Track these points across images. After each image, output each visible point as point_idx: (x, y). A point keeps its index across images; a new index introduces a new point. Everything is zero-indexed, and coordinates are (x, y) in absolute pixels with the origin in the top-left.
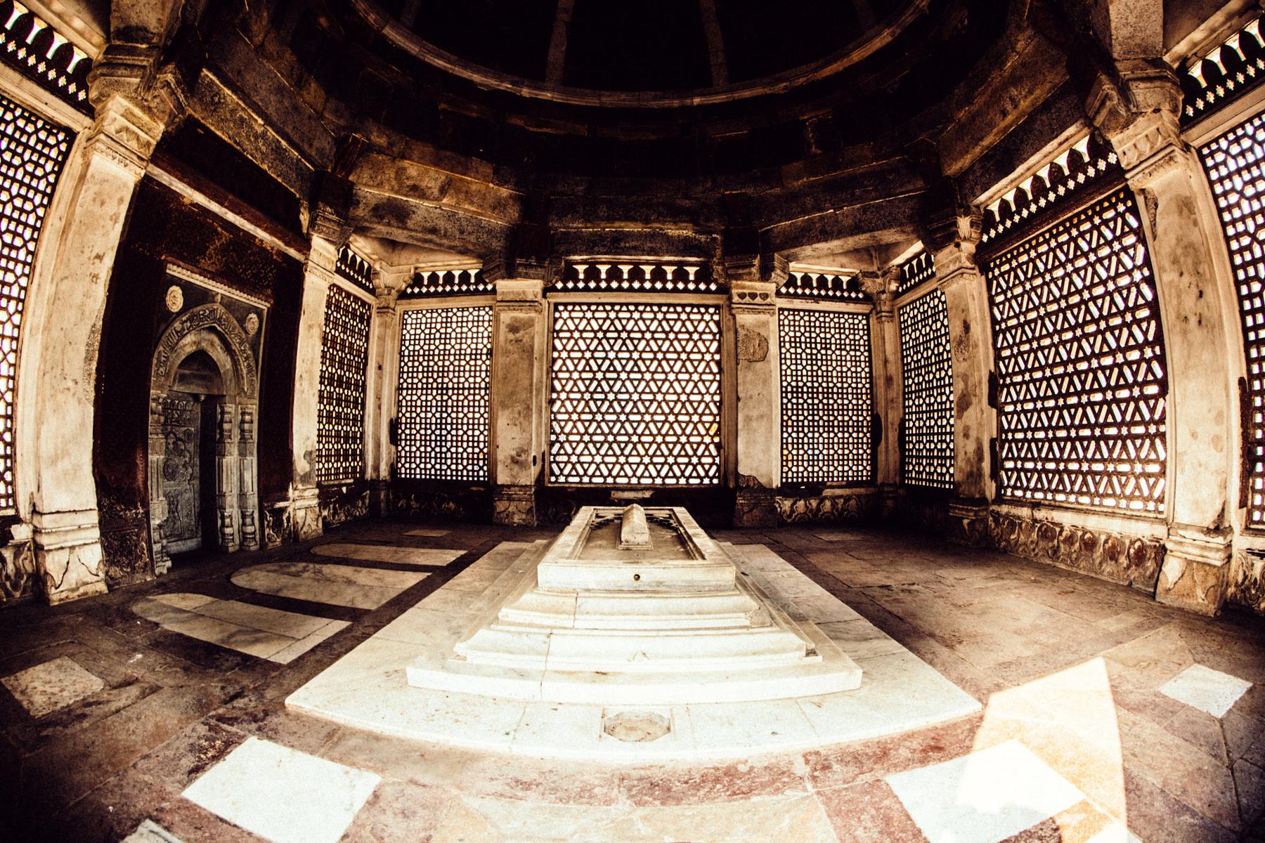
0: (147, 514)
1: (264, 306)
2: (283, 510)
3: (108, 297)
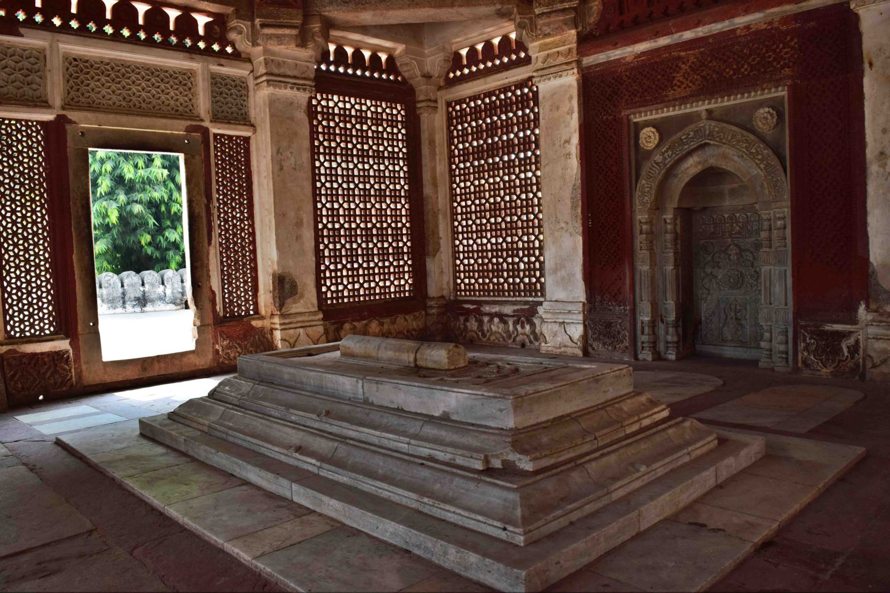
0: (633, 311)
1: (782, 93)
2: (843, 335)
3: (581, 164)
